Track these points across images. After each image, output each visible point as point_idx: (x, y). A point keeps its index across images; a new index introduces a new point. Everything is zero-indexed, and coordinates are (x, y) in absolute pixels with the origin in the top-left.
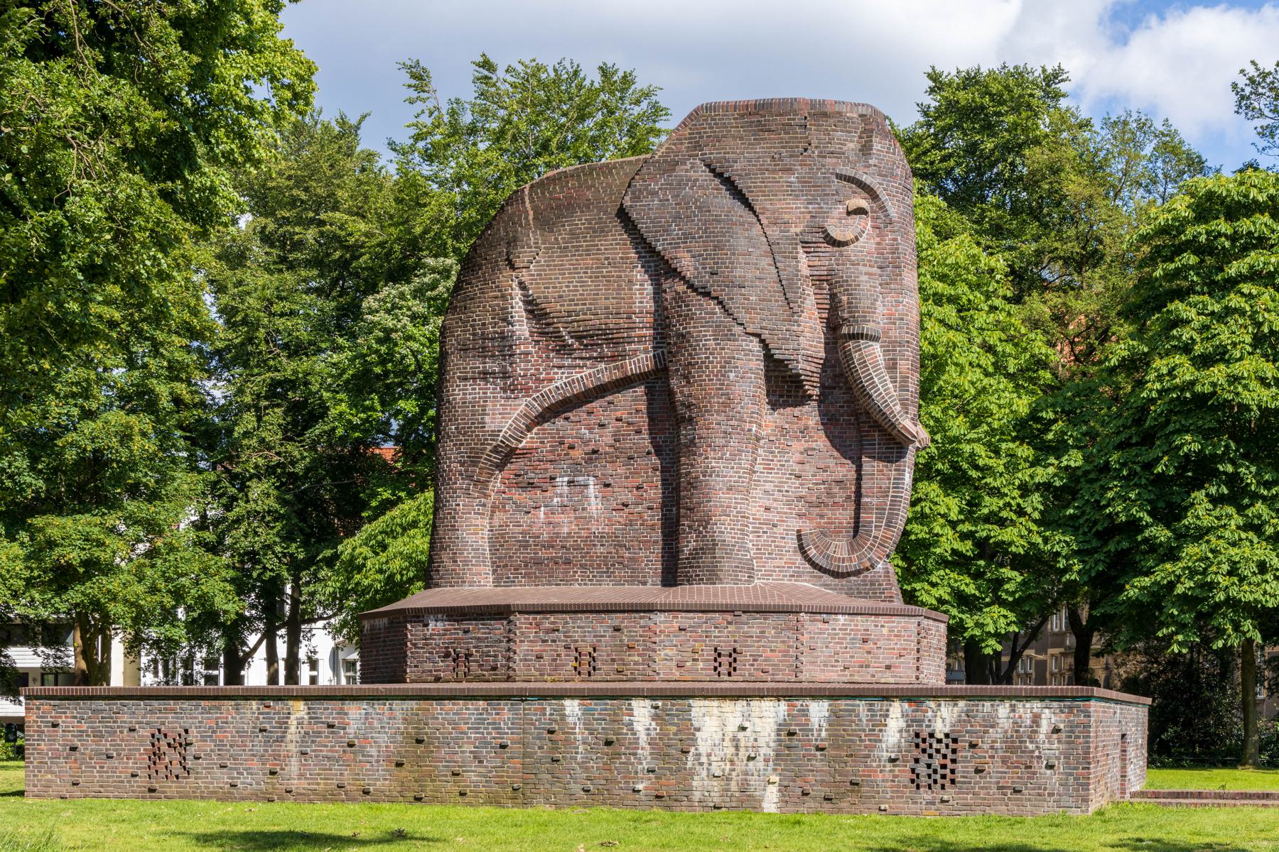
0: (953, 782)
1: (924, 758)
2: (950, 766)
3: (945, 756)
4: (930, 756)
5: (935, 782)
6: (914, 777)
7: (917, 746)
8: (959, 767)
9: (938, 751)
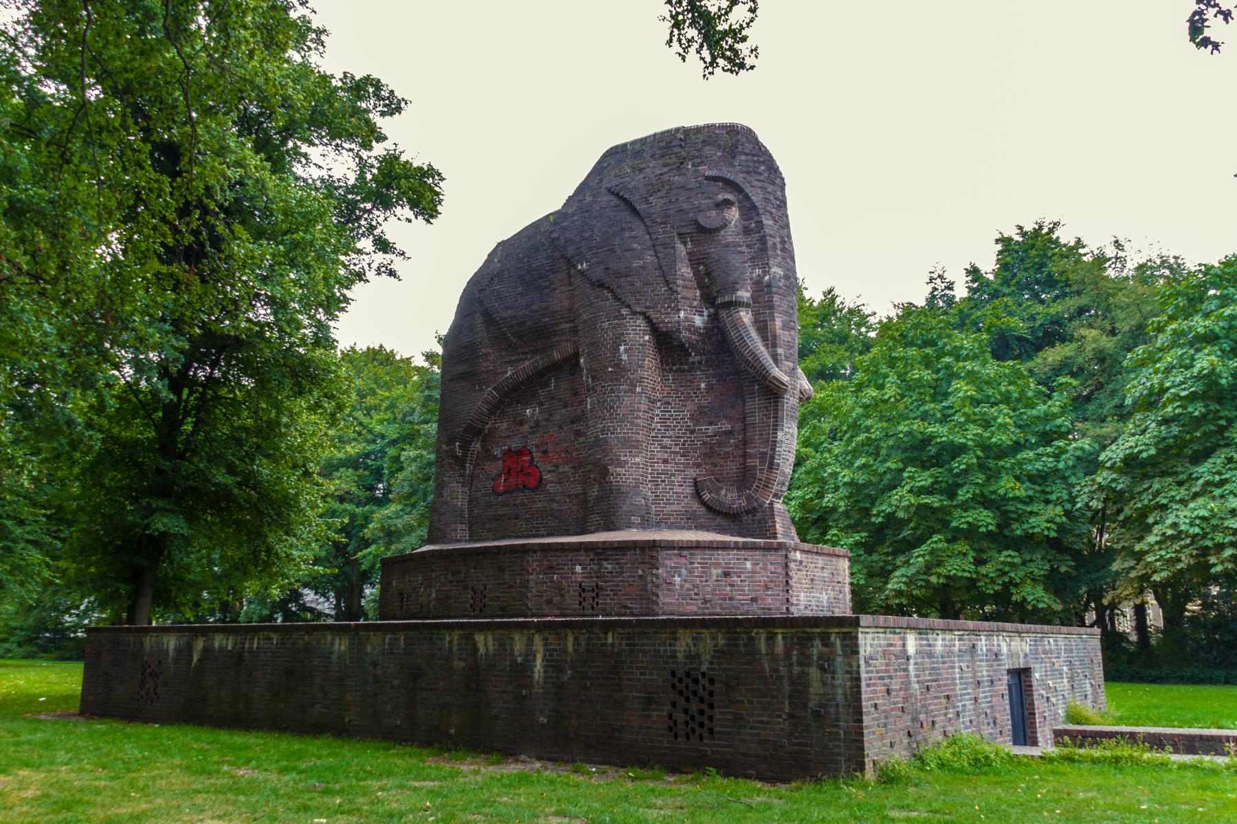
0: (711, 731)
1: (681, 702)
2: (708, 712)
3: (702, 700)
4: (687, 699)
5: (693, 730)
6: (672, 723)
7: (674, 686)
8: (717, 714)
9: (695, 693)
